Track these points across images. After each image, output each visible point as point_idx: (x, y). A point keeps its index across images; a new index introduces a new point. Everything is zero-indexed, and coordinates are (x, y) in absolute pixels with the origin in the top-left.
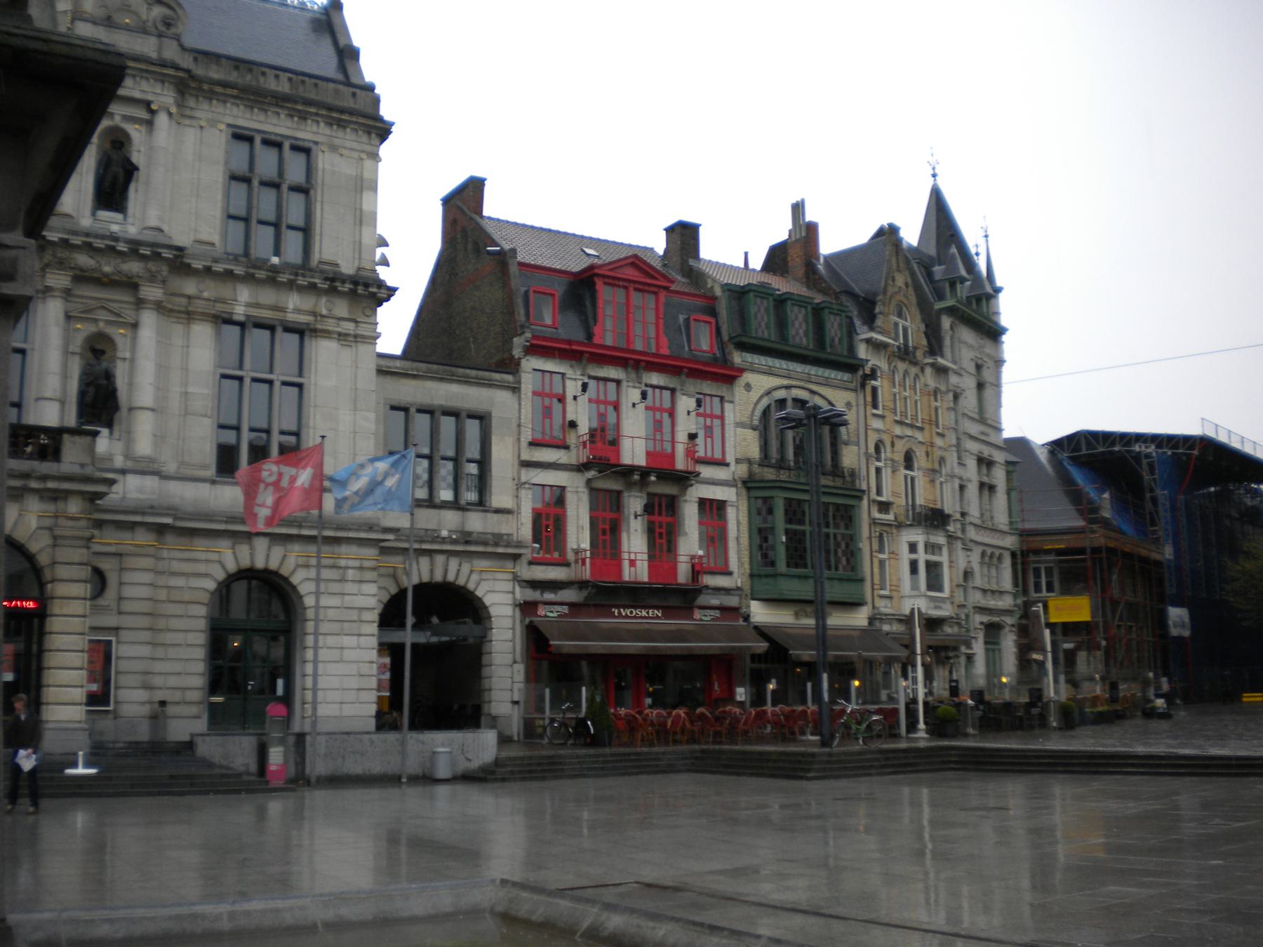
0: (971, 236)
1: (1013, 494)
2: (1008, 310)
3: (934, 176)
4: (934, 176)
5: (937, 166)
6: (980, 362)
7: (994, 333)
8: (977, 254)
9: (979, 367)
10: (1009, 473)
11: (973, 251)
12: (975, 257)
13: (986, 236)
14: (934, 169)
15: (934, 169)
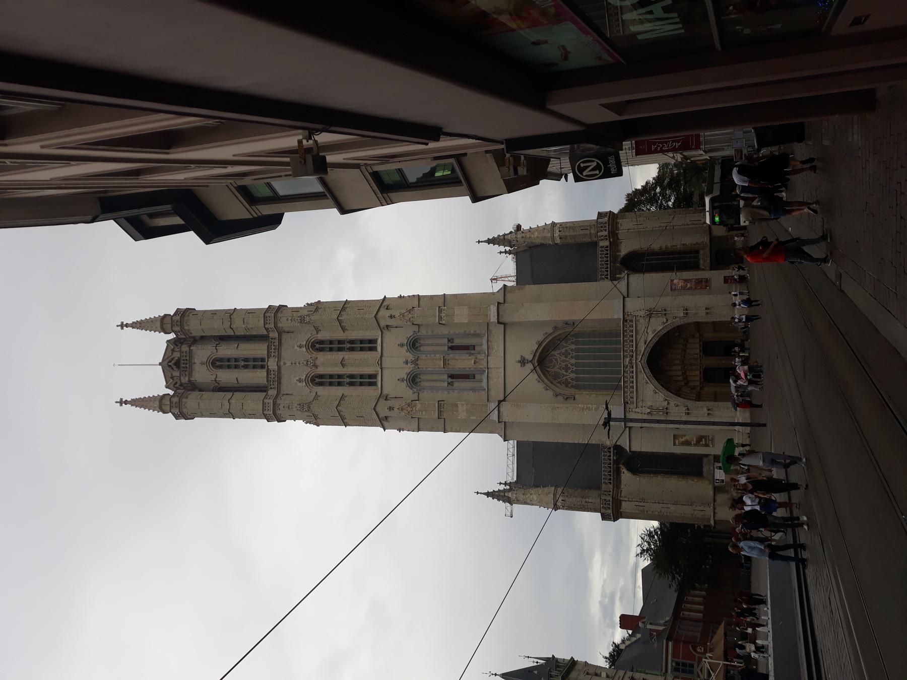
0: (529, 664)
1: (647, 671)
2: (563, 655)
3: (496, 675)
4: (496, 675)
5: (492, 673)
6: (586, 672)
7: (573, 663)
8: (537, 662)
9: (588, 674)
10: (637, 671)
11: (535, 664)
12: (539, 664)
13: (528, 657)
14: (493, 674)
15: (493, 674)
